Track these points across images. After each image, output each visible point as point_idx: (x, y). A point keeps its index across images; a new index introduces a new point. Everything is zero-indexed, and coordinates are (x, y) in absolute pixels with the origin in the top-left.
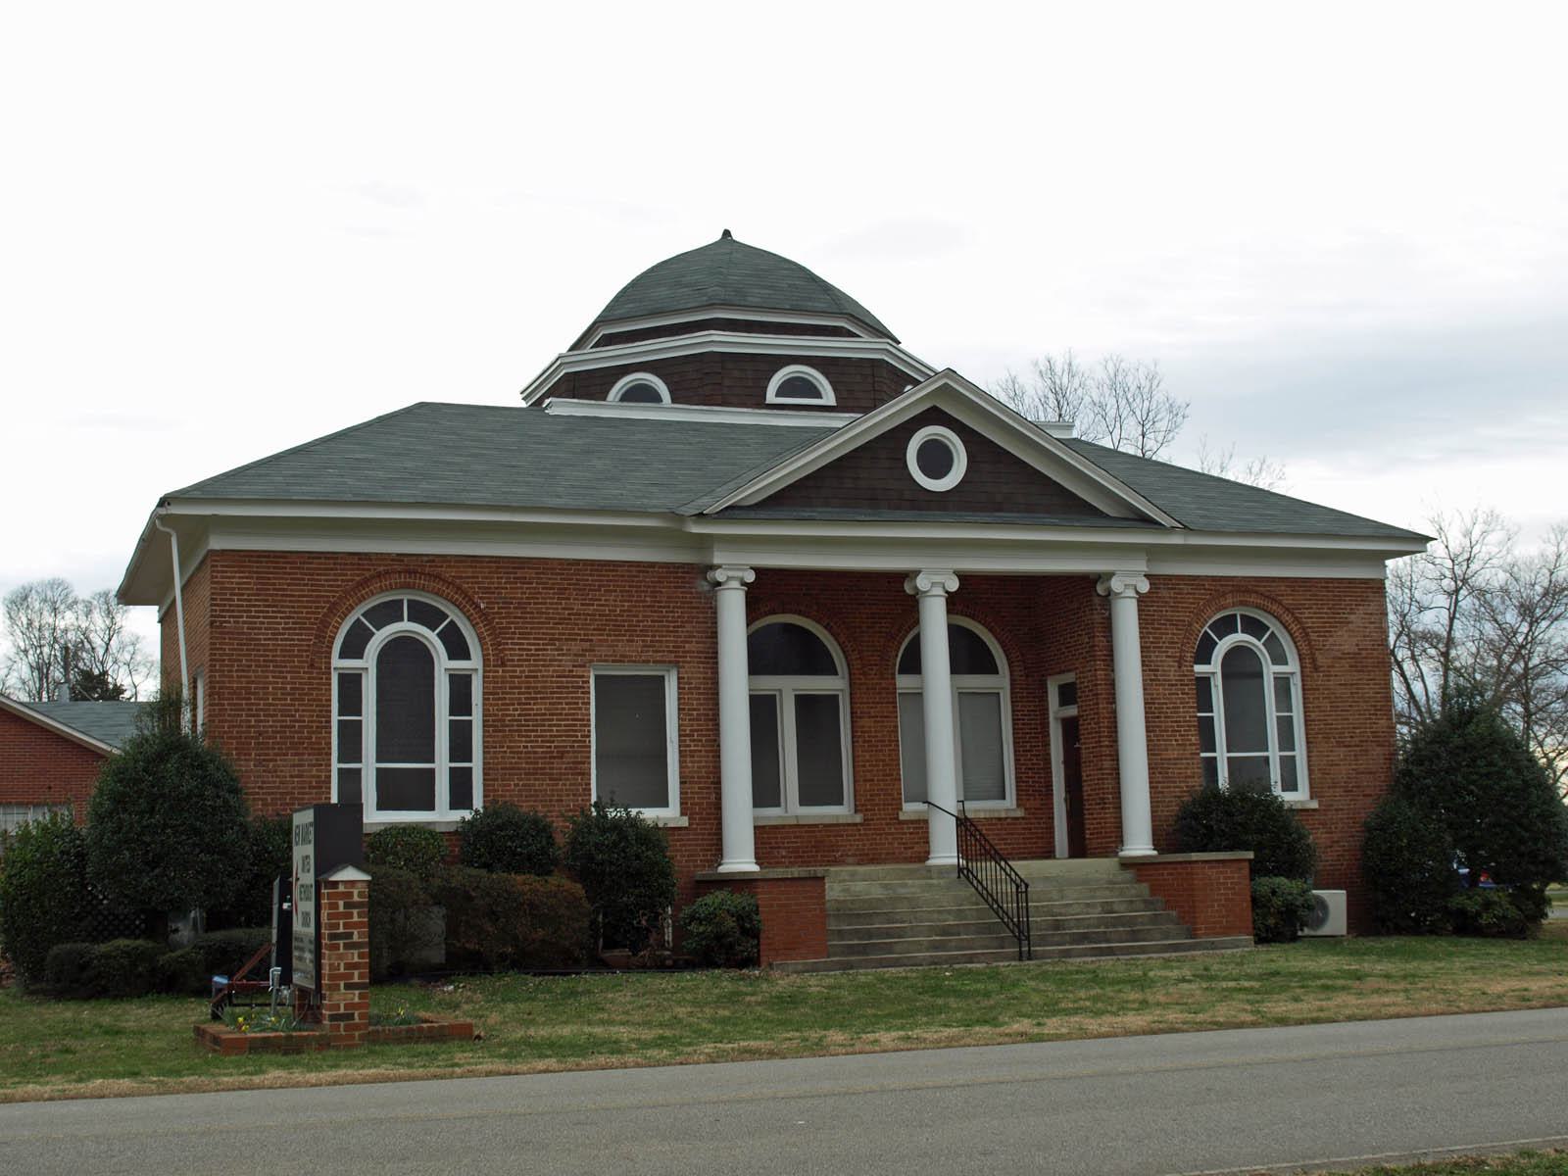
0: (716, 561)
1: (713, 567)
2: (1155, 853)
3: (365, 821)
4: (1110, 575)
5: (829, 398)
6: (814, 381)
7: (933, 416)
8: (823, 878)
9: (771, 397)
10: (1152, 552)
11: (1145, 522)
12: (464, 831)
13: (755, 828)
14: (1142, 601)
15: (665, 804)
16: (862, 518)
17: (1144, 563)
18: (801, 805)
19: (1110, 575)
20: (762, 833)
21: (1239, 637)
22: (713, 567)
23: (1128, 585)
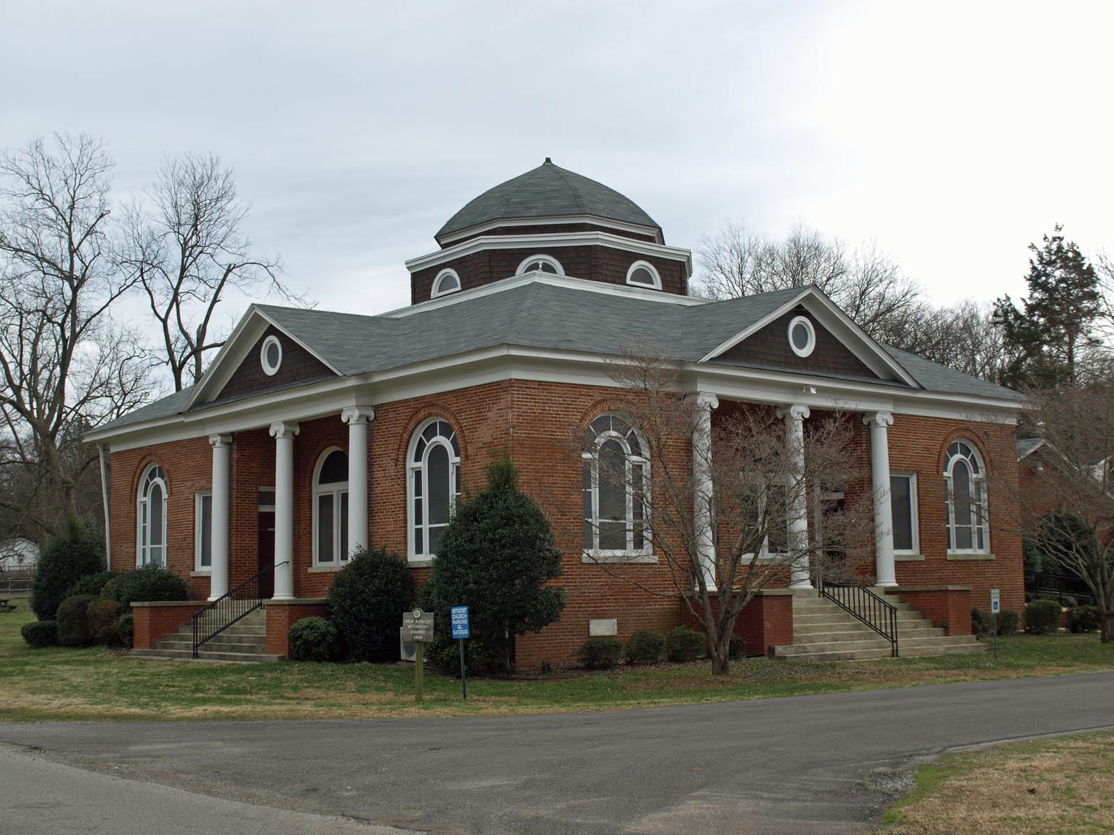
0: (699, 390)
1: (697, 394)
2: (897, 585)
3: (409, 560)
4: (875, 413)
5: (658, 284)
6: (652, 276)
7: (799, 310)
8: (791, 596)
9: (629, 281)
10: (896, 400)
11: (896, 381)
12: (346, 570)
13: (895, 562)
14: (889, 428)
15: (910, 547)
16: (746, 365)
17: (892, 406)
18: (332, 560)
19: (875, 413)
20: (900, 565)
21: (958, 456)
22: (697, 394)
23: (884, 416)
